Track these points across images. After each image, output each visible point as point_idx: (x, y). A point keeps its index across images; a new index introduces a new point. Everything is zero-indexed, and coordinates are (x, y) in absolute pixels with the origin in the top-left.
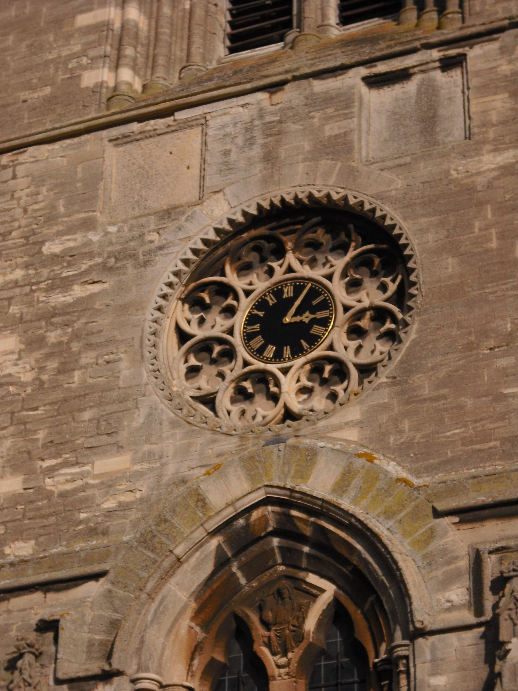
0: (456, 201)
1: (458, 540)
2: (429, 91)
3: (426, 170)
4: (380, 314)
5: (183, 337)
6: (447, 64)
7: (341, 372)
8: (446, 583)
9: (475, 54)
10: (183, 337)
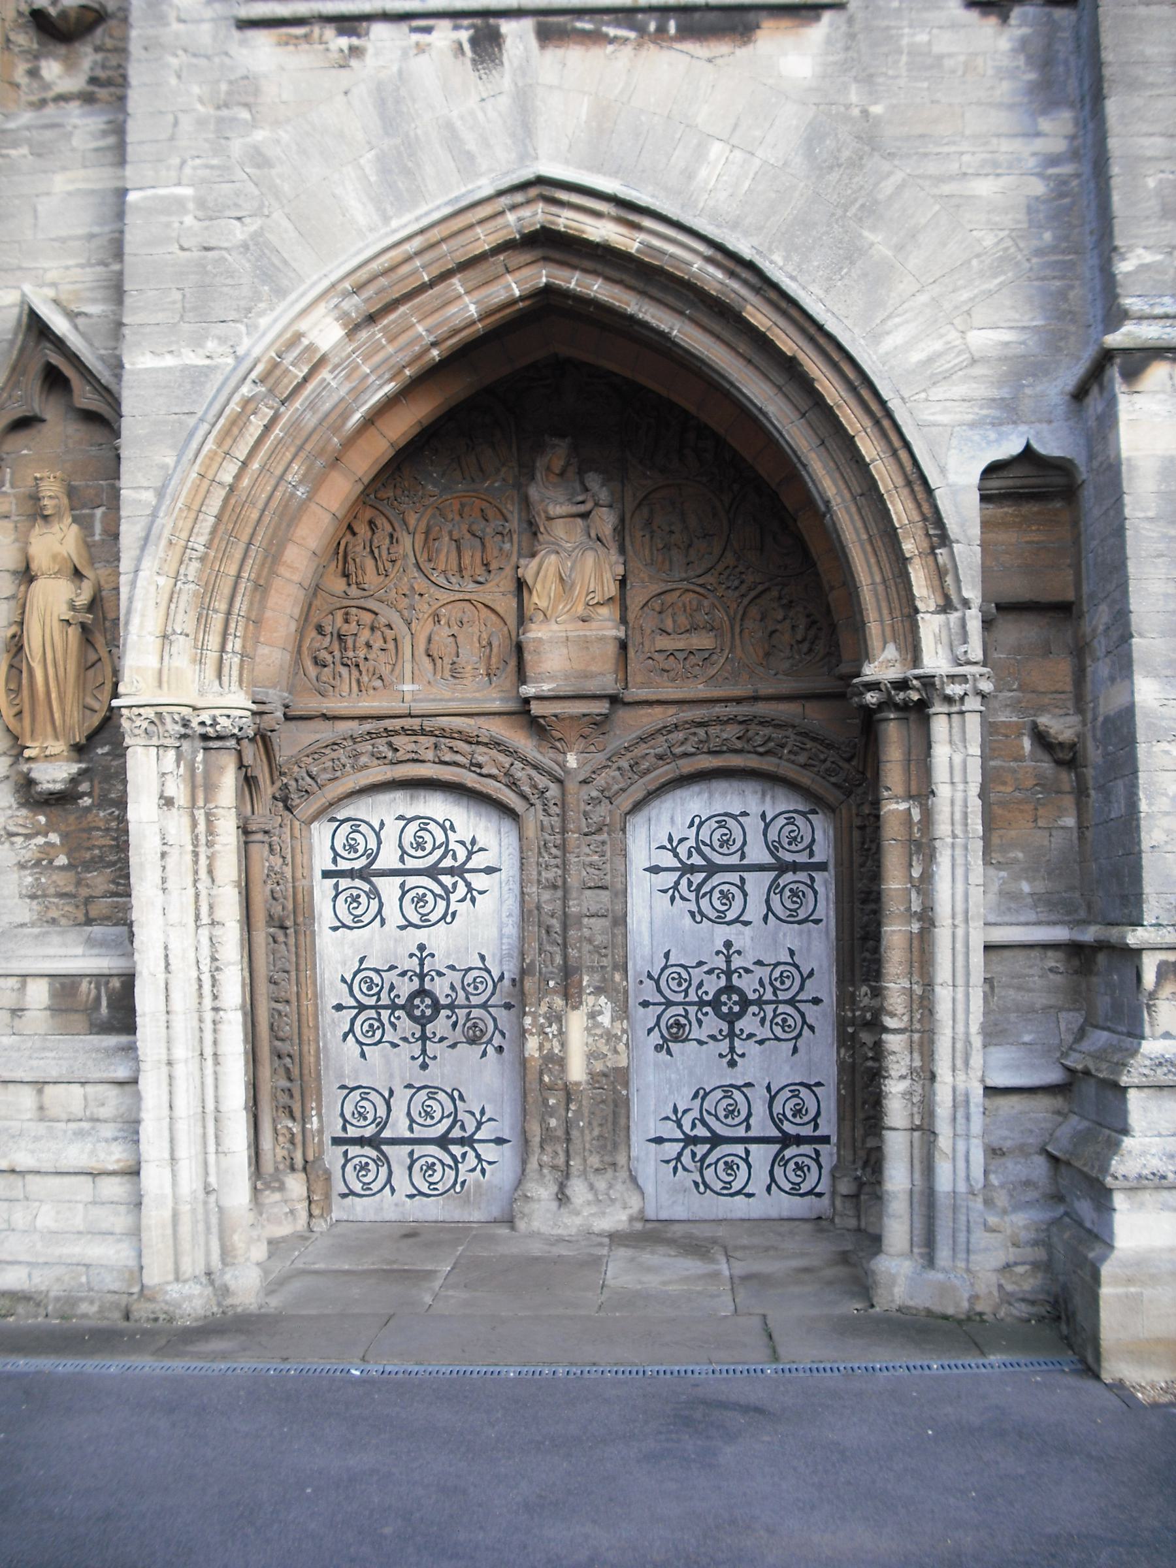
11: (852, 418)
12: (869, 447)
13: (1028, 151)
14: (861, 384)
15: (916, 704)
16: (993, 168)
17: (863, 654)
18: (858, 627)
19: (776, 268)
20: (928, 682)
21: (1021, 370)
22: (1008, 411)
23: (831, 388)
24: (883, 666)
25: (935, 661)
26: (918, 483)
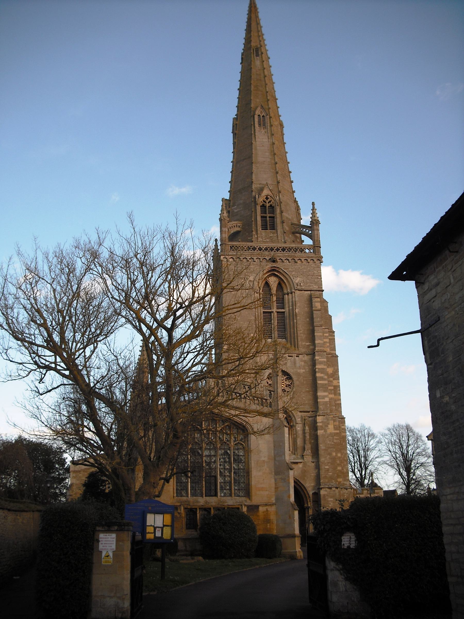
0: (299, 375)
1: (300, 414)
2: (295, 359)
3: (295, 370)
4: (289, 385)
5: (268, 383)
6: (297, 356)
7: (285, 391)
8: (298, 418)
9: (300, 356)
10: (268, 383)
11: (304, 490)
12: (305, 492)
13: (315, 472)
14: (305, 488)
15: (308, 508)
16: (313, 473)
17: (304, 504)
18: (304, 502)
19: (299, 480)
20: (309, 507)
21: (314, 487)
22: (314, 489)
23: (303, 488)
24: (306, 505)
25: (309, 505)
26: (308, 494)
